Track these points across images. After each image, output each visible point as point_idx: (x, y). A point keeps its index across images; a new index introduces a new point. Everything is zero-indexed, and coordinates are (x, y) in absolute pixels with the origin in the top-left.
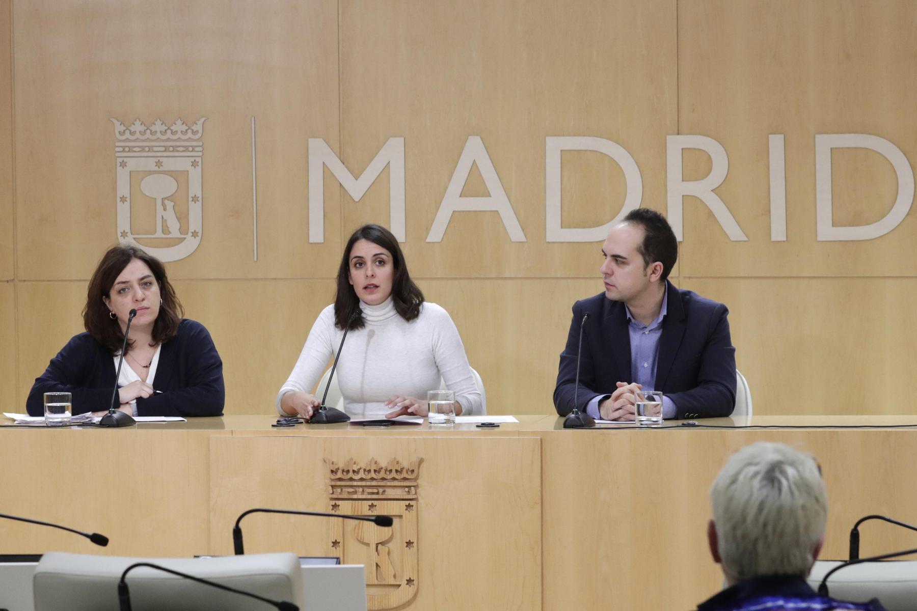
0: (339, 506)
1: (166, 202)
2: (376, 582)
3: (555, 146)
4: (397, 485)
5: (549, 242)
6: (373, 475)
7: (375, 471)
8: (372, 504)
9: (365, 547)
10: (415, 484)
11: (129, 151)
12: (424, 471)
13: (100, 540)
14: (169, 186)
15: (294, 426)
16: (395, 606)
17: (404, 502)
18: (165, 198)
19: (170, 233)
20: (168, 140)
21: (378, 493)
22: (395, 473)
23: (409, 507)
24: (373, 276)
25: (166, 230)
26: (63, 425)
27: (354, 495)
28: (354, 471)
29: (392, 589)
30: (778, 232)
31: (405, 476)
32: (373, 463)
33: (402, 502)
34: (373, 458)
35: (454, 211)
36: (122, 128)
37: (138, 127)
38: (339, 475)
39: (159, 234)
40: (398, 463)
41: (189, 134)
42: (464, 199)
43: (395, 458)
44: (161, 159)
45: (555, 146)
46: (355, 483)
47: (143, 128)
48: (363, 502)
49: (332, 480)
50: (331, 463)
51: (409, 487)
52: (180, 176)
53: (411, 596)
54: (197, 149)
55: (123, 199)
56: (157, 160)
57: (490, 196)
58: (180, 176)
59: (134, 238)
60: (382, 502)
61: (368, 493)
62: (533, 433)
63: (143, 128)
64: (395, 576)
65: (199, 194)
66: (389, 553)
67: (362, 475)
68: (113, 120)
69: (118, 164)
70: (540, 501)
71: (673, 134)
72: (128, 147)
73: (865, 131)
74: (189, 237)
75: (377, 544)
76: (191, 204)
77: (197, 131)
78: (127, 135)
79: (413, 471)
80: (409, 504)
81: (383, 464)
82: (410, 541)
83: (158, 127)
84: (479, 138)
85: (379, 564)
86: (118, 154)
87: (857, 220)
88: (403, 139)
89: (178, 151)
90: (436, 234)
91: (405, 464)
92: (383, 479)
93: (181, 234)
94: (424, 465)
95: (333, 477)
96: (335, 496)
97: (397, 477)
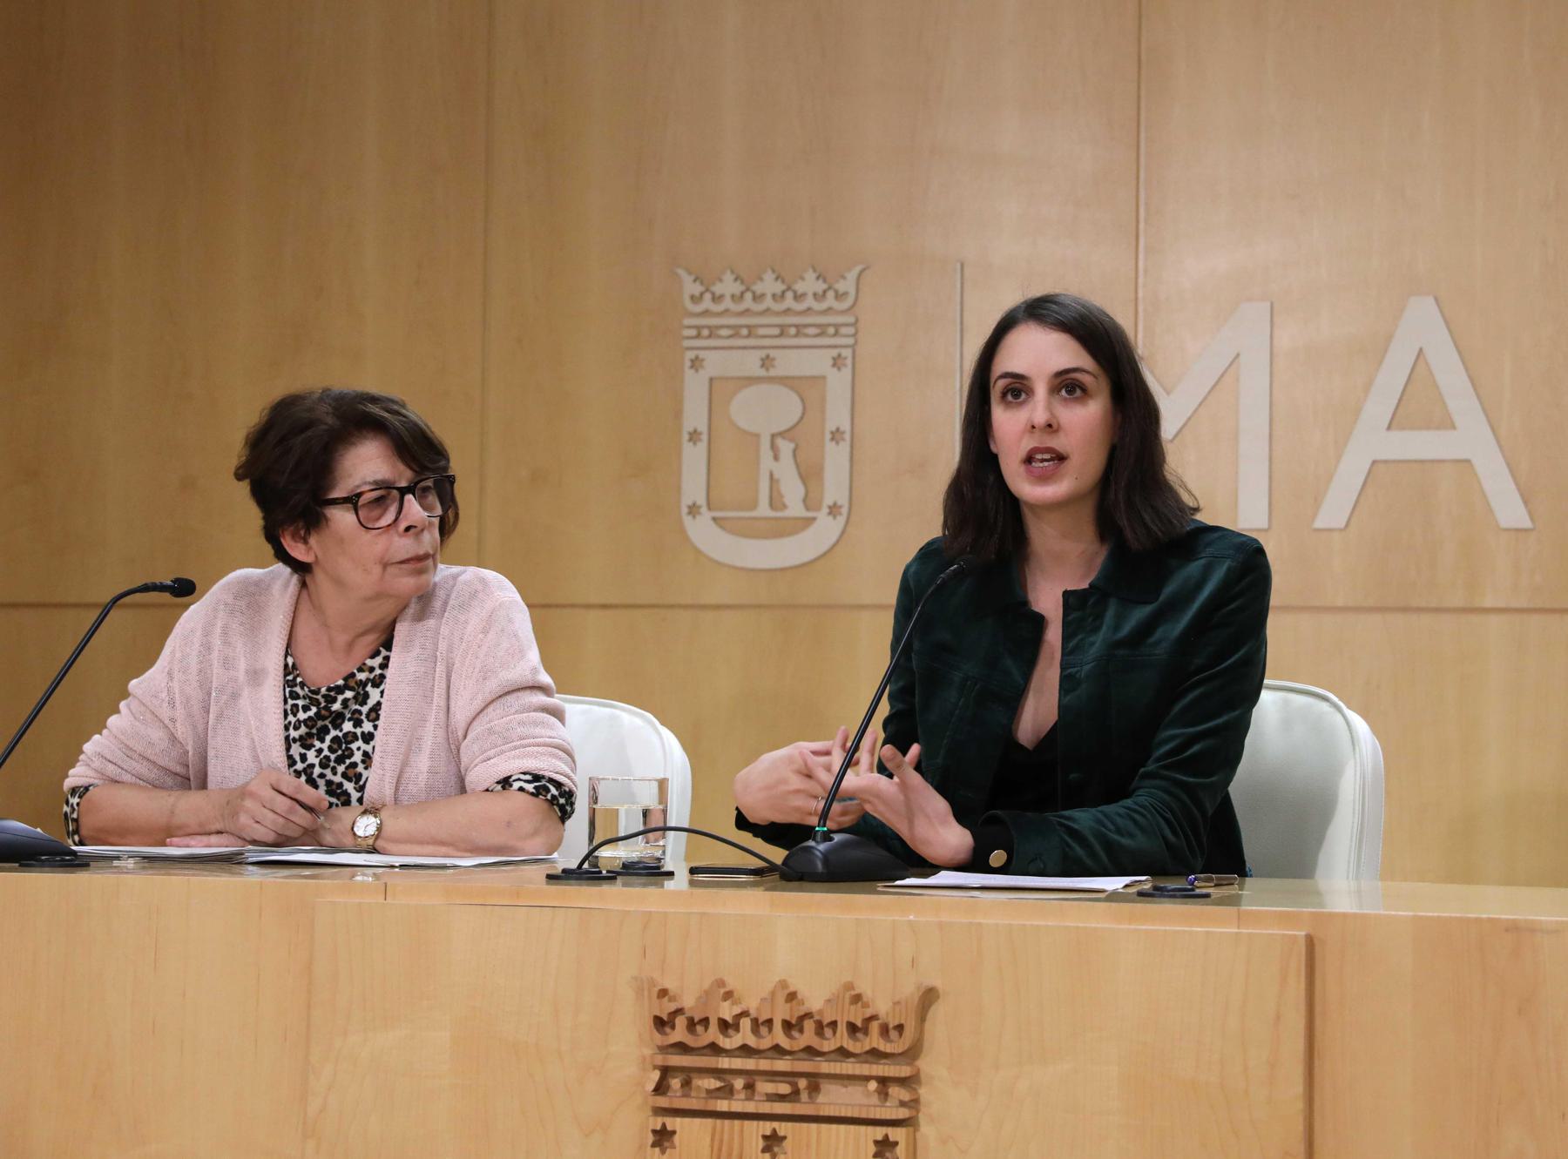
0: (674, 1132)
1: (780, 442)
4: (857, 1072)
6: (779, 1037)
7: (788, 1026)
8: (774, 1131)
10: (904, 1071)
11: (710, 336)
14: (784, 408)
17: (870, 1129)
18: (781, 434)
19: (785, 507)
20: (787, 311)
21: (794, 1096)
25: (776, 501)
28: (724, 1026)
31: (876, 1046)
32: (781, 997)
33: (863, 1128)
34: (783, 984)
35: (1374, 462)
36: (697, 289)
37: (728, 286)
38: (679, 1034)
39: (764, 510)
40: (857, 999)
41: (830, 301)
42: (1396, 435)
43: (849, 986)
44: (772, 353)
46: (724, 1063)
47: (737, 288)
48: (747, 1123)
49: (664, 1049)
50: (655, 995)
51: (884, 1081)
52: (806, 387)
54: (843, 330)
55: (694, 436)
56: (763, 353)
57: (1453, 427)
58: (806, 387)
59: (714, 519)
60: (805, 1125)
61: (767, 1094)
63: (737, 288)
65: (846, 427)
67: (745, 1036)
68: (681, 272)
69: (688, 364)
72: (709, 327)
74: (822, 516)
76: (830, 447)
77: (846, 294)
79: (900, 1028)
80: (886, 1136)
81: (815, 1000)
83: (769, 285)
84: (1431, 300)
86: (686, 343)
88: (1269, 304)
89: (807, 336)
90: (1333, 512)
92: (810, 1051)
93: (808, 509)
96: (663, 1102)
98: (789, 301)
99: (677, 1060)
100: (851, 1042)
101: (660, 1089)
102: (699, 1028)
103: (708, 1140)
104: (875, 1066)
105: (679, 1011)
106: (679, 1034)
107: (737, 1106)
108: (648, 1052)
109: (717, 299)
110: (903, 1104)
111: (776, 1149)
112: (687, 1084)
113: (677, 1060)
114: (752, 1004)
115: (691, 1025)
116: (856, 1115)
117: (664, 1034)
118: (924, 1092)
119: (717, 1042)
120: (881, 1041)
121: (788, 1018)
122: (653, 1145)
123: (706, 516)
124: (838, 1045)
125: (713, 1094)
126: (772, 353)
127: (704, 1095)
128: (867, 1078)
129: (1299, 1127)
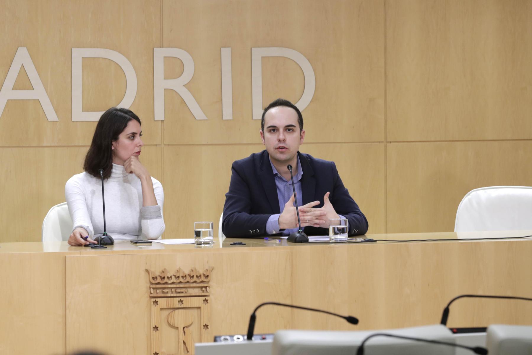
4: (196, 286)
5: (74, 122)
6: (181, 279)
8: (181, 300)
12: (213, 276)
13: (353, 321)
15: (106, 248)
17: (202, 297)
24: (284, 140)
26: (342, 242)
28: (168, 278)
30: (228, 114)
31: (202, 280)
35: (8, 100)
38: (159, 280)
46: (169, 286)
60: (187, 298)
67: (173, 279)
71: (157, 47)
73: (282, 45)
79: (208, 276)
81: (187, 272)
84: (25, 48)
85: (185, 341)
92: (188, 282)
95: (153, 282)
102: (155, 279)
103: (166, 302)
104: (193, 285)
108: (148, 285)
116: (199, 295)
119: (167, 282)
124: (194, 280)
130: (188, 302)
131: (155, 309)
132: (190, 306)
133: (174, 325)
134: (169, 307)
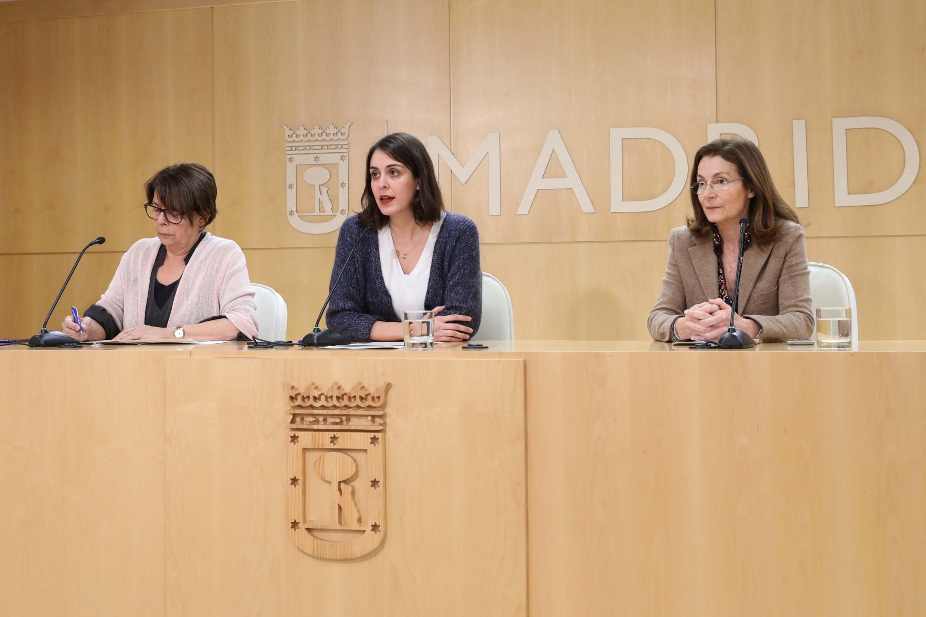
0: (298, 437)
1: (322, 187)
2: (338, 527)
3: (617, 135)
6: (335, 402)
7: (338, 398)
8: (334, 435)
9: (328, 485)
10: (380, 413)
11: (295, 150)
14: (324, 175)
16: (359, 556)
17: (369, 433)
19: (325, 211)
22: (359, 400)
23: (374, 440)
25: (321, 209)
27: (314, 425)
28: (315, 398)
29: (357, 535)
31: (370, 404)
32: (336, 387)
33: (366, 433)
38: (299, 402)
39: (317, 212)
40: (363, 388)
43: (360, 383)
44: (318, 155)
45: (617, 135)
46: (316, 412)
47: (305, 132)
48: (324, 433)
49: (294, 408)
50: (290, 388)
51: (373, 417)
52: (329, 167)
53: (376, 545)
54: (344, 147)
55: (291, 186)
56: (315, 156)
57: (566, 177)
60: (345, 433)
62: (517, 354)
63: (305, 132)
64: (360, 520)
65: (346, 182)
66: (353, 493)
67: (322, 402)
68: (284, 126)
70: (523, 436)
75: (340, 483)
78: (294, 137)
79: (379, 397)
81: (347, 389)
82: (375, 479)
83: (317, 131)
84: (557, 130)
87: (869, 189)
90: (523, 209)
91: (372, 390)
92: (346, 407)
94: (392, 392)
96: (294, 426)
97: (361, 404)
98: (324, 136)
99: (298, 411)
100: (361, 403)
101: (293, 422)
102: (306, 400)
104: (370, 411)
105: (299, 394)
106: (299, 402)
107: (321, 427)
108: (288, 408)
109: (297, 136)
110: (380, 424)
111: (335, 442)
112: (302, 419)
113: (298, 411)
114: (325, 391)
115: (303, 398)
116: (364, 429)
117: (293, 402)
118: (388, 420)
120: (372, 403)
121: (338, 395)
122: (291, 442)
123: (296, 215)
125: (311, 423)
126: (318, 155)
127: (309, 423)
128: (367, 416)
129: (522, 429)
130: (345, 440)
131: (296, 448)
132: (349, 448)
133: (324, 478)
134: (316, 447)
